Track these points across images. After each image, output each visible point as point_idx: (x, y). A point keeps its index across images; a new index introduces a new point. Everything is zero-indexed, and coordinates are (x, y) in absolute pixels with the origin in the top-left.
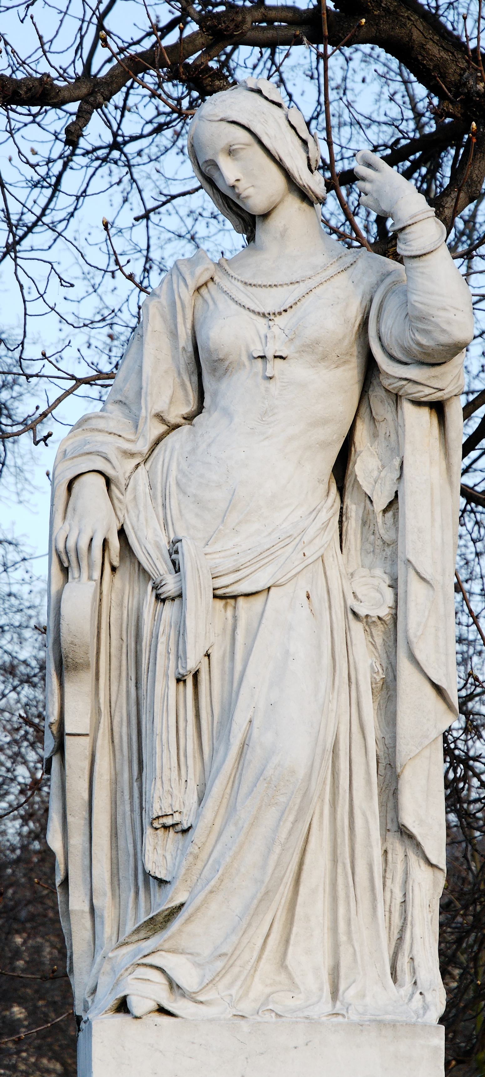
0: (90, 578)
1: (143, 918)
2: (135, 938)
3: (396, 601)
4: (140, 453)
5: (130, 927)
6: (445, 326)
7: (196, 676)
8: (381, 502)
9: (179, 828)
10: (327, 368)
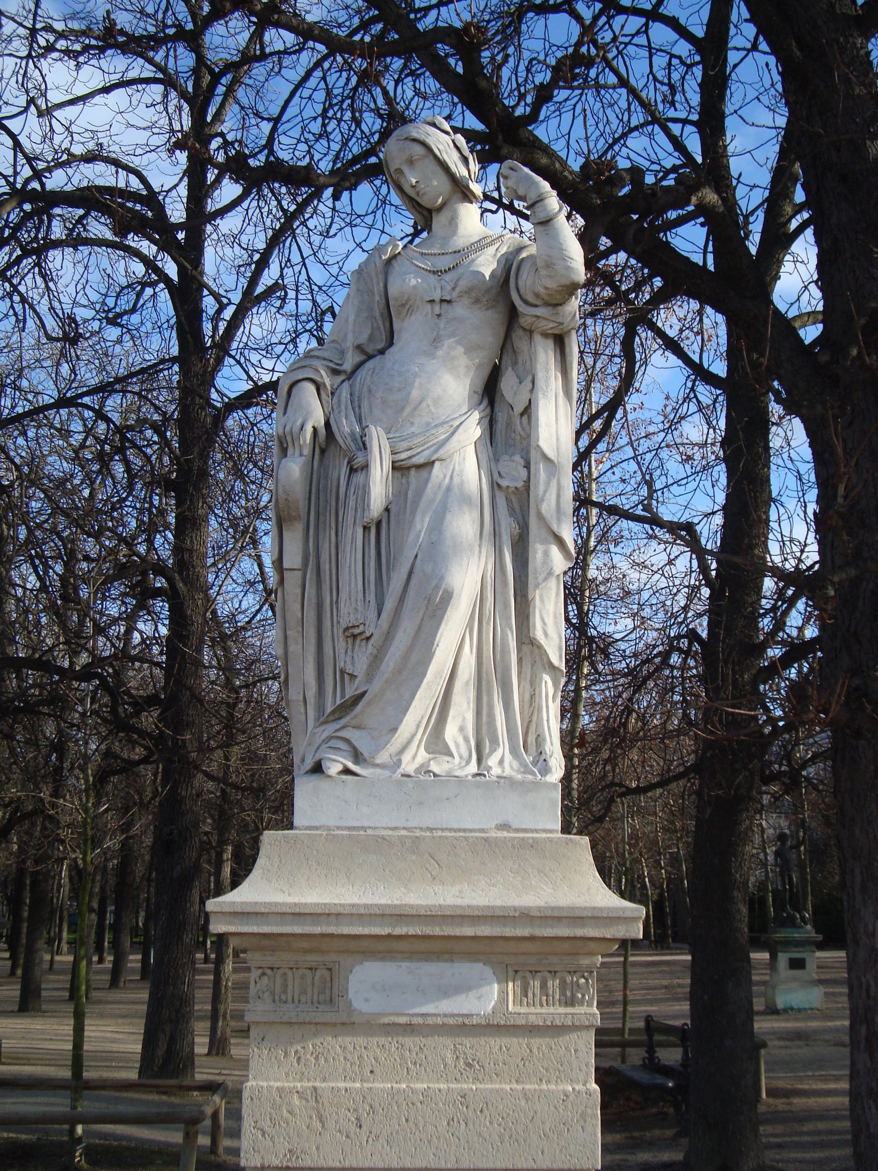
0: (301, 455)
1: (338, 702)
2: (332, 718)
3: (529, 477)
4: (345, 372)
5: (329, 709)
7: (379, 524)
8: (519, 409)
9: (363, 636)
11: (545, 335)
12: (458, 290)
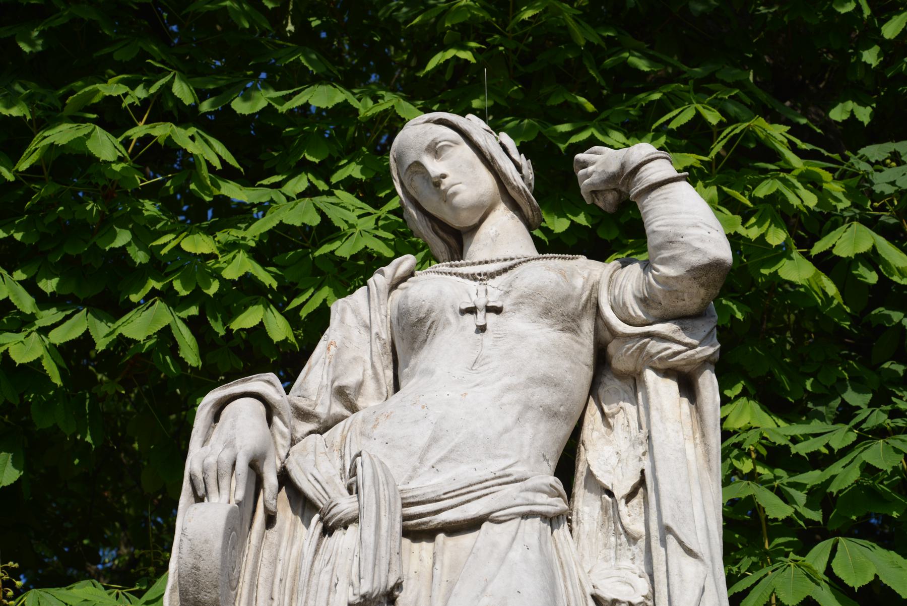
6: (698, 244)
10: (551, 326)
11: (666, 373)
12: (514, 295)
